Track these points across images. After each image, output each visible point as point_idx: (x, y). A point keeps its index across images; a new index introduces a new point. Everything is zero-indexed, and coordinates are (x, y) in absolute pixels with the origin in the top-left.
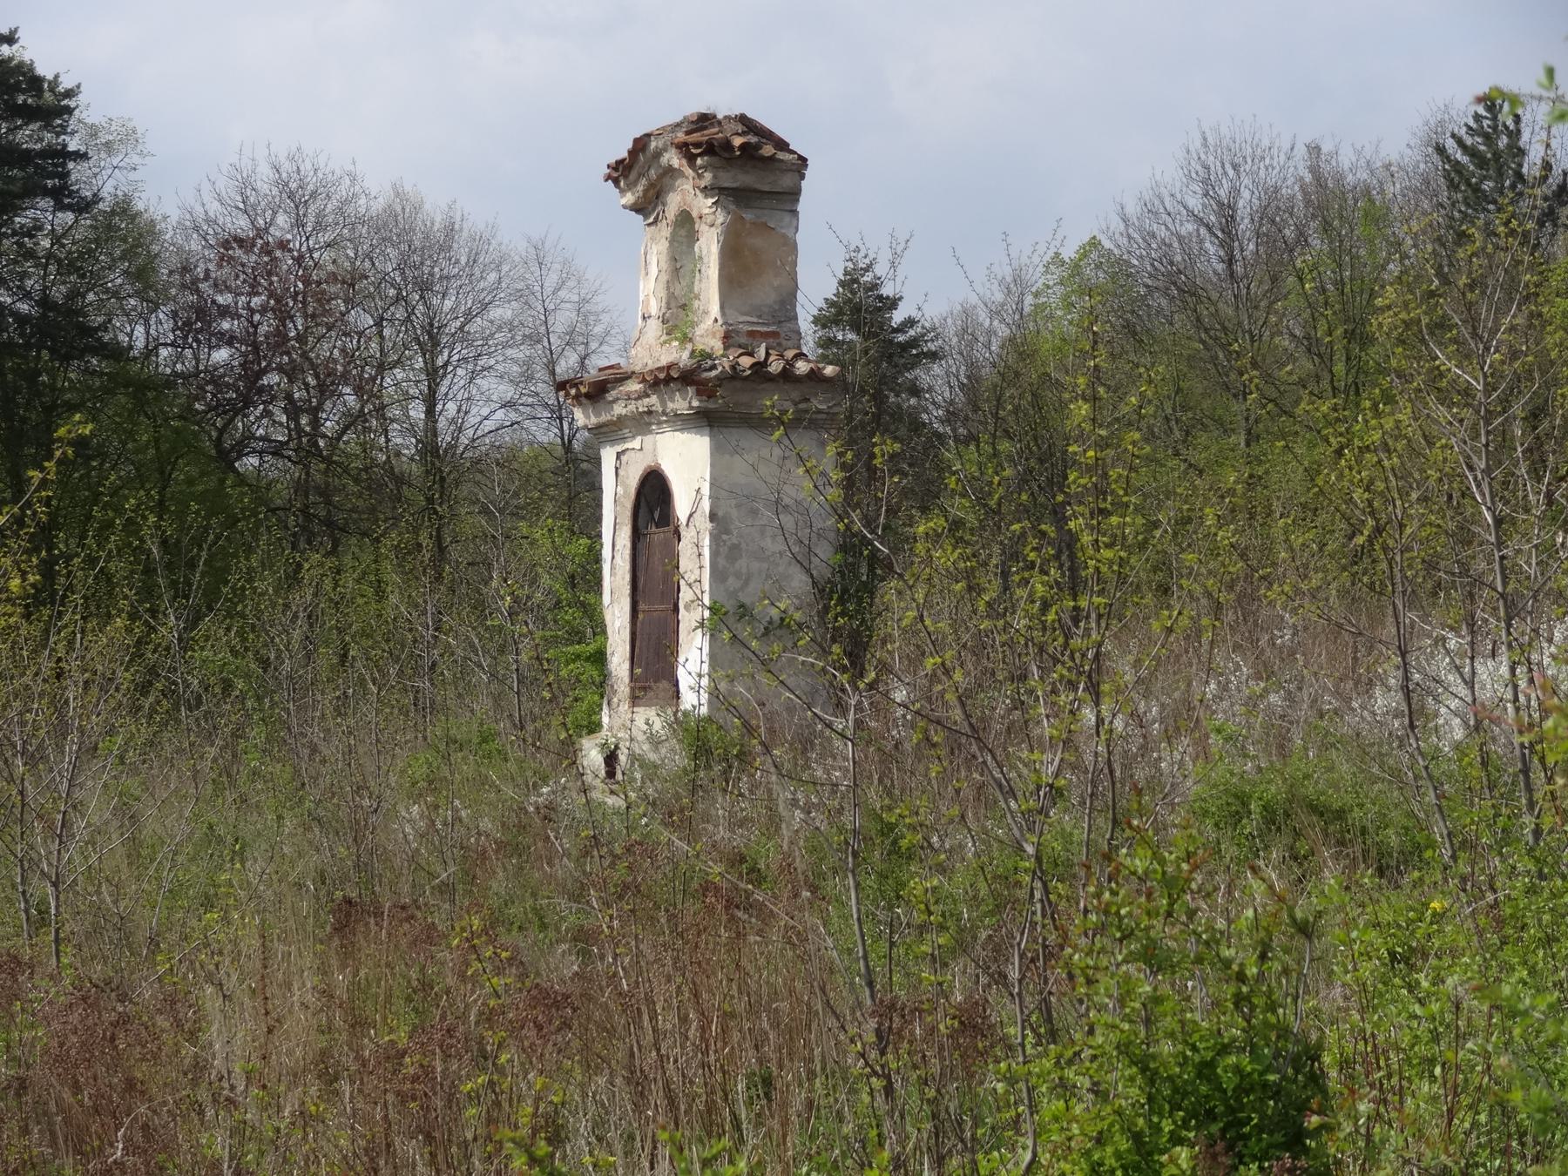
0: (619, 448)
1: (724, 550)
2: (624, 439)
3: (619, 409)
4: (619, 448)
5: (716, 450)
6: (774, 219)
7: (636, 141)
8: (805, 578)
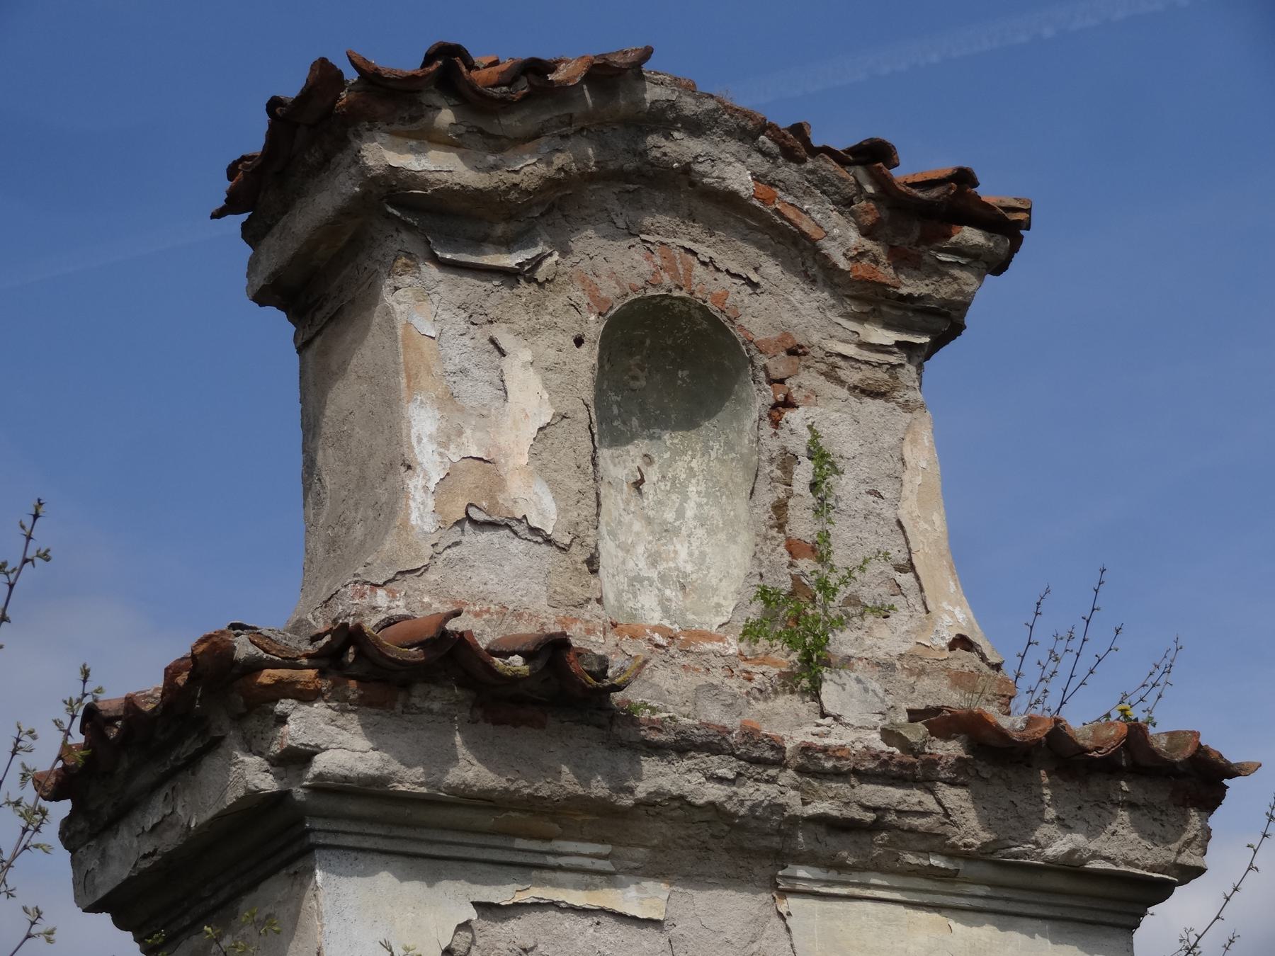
0: (503, 894)
2: (526, 869)
3: (658, 777)
4: (503, 894)
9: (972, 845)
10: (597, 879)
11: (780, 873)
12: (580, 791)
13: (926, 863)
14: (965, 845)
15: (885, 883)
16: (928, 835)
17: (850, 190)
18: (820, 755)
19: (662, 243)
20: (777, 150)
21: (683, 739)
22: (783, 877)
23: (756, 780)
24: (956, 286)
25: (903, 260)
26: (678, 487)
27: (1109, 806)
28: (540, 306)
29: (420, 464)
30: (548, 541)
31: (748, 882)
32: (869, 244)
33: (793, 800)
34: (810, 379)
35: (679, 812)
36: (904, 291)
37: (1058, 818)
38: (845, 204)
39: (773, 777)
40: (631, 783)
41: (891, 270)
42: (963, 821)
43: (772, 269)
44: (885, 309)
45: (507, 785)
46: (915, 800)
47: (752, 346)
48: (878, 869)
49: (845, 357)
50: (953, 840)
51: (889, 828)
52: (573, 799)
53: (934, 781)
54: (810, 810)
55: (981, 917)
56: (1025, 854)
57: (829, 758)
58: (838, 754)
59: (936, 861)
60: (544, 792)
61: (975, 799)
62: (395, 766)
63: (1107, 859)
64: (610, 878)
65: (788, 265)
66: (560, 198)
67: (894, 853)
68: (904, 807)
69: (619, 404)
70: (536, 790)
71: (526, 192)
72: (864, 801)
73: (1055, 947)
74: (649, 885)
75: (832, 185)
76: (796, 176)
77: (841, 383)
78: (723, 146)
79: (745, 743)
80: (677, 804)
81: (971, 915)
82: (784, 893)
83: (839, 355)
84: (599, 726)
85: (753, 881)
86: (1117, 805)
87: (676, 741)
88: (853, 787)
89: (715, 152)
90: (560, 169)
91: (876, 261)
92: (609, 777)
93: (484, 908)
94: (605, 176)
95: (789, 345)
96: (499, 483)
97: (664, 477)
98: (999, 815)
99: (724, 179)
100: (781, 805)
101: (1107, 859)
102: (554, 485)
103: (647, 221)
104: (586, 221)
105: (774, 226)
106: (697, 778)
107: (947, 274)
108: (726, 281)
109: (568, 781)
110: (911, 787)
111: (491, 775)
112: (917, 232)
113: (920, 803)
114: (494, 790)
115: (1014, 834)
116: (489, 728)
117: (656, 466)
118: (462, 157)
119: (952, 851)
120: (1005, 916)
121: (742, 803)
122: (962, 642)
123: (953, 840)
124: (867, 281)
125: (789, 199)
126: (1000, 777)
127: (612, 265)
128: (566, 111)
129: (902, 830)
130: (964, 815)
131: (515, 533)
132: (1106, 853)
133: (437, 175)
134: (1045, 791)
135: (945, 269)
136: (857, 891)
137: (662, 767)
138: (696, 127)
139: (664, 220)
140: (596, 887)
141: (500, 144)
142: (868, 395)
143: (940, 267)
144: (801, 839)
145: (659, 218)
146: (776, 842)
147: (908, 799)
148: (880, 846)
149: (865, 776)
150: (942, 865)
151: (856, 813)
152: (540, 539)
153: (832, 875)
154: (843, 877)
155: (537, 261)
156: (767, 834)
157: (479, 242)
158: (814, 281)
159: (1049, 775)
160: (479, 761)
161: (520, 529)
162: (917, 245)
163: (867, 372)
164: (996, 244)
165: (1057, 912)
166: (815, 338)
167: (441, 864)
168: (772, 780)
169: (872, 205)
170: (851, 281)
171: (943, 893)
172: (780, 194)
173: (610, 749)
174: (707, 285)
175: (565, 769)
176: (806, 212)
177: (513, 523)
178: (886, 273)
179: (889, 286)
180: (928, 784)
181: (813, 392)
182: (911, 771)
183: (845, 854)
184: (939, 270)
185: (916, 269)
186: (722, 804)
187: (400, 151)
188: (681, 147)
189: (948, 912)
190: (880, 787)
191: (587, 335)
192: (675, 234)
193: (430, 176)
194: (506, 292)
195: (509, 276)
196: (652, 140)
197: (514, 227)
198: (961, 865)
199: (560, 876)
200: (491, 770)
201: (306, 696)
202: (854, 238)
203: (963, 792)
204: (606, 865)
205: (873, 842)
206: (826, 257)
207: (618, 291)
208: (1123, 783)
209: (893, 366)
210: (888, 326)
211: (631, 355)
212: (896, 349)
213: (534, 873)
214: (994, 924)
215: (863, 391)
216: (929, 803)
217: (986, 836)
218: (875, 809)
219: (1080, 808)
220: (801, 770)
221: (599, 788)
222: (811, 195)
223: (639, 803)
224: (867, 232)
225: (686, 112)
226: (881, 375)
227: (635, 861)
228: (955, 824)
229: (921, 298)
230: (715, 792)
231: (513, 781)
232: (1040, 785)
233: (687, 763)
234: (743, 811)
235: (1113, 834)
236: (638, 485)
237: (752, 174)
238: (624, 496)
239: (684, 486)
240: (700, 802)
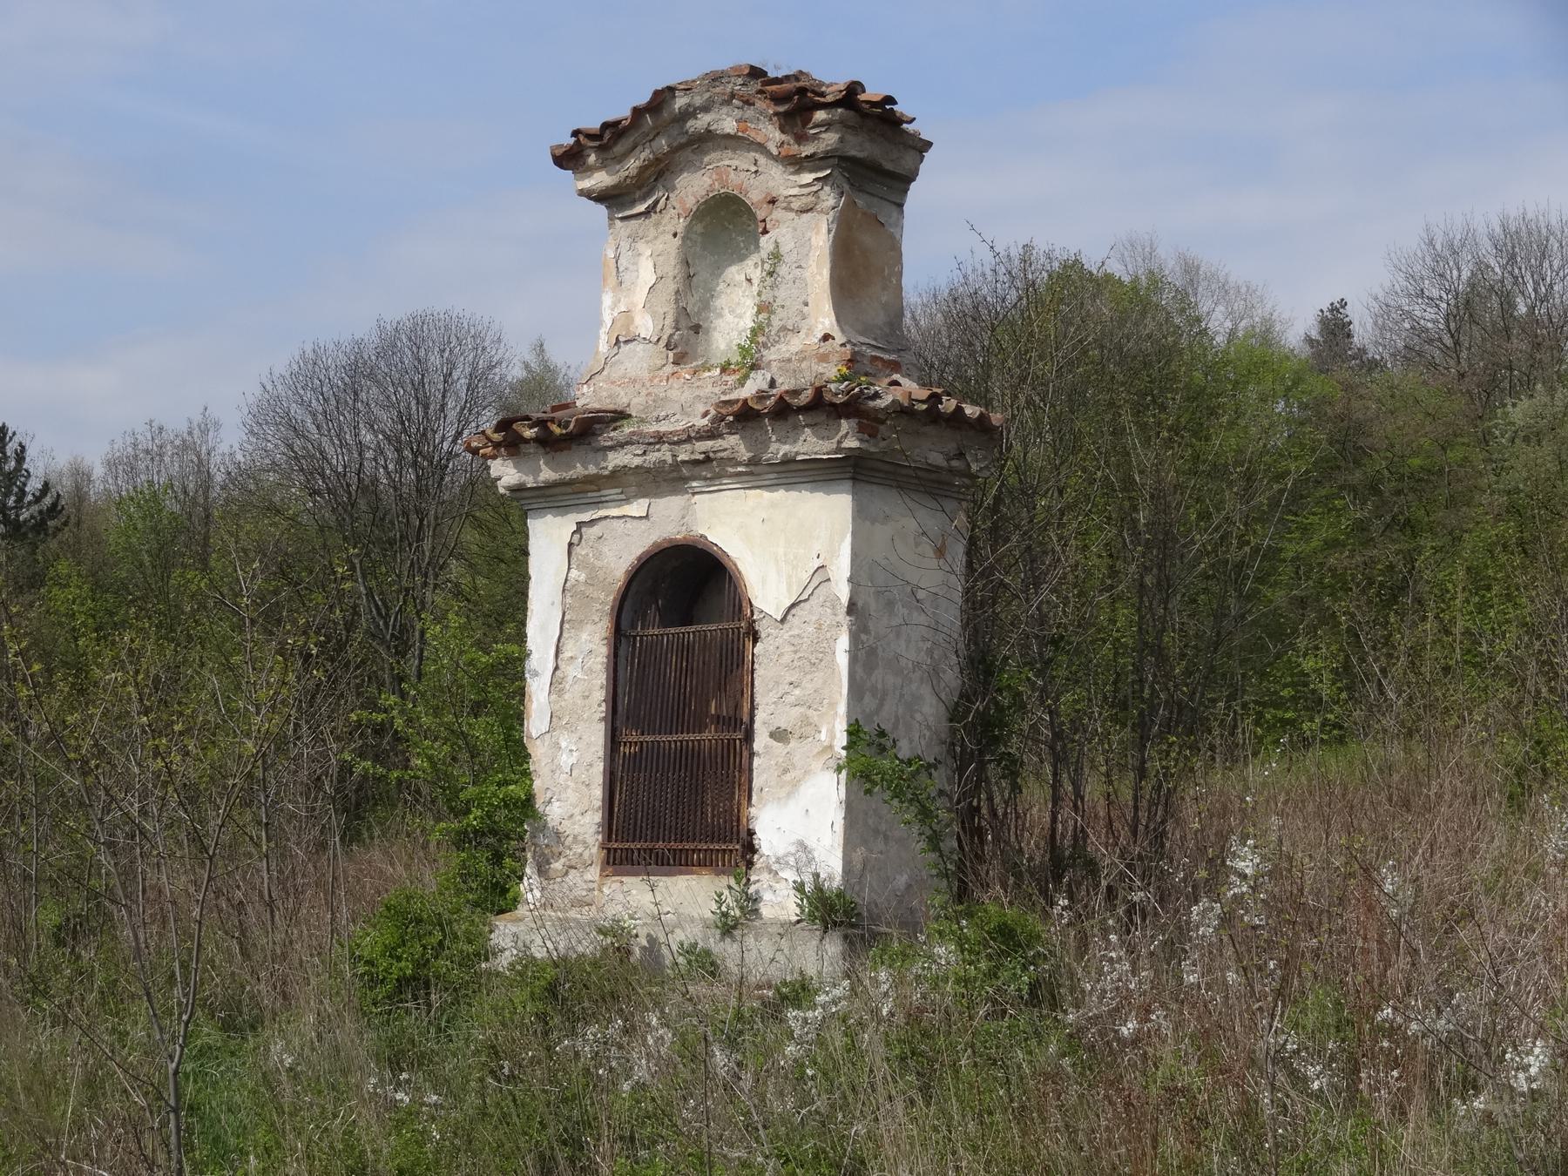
0: (586, 517)
1: (862, 655)
2: (598, 504)
3: (616, 459)
4: (586, 517)
5: (860, 514)
6: (885, 213)
7: (657, 93)
8: (934, 700)
25: (801, 139)
28: (657, 224)
34: (778, 214)
62: (524, 478)
64: (627, 500)
77: (792, 210)
93: (580, 525)
94: (675, 150)
103: (706, 159)
104: (682, 171)
106: (629, 456)
108: (743, 175)
120: (789, 486)
122: (826, 337)
127: (693, 187)
138: (706, 109)
139: (713, 155)
141: (621, 159)
155: (656, 202)
157: (633, 203)
163: (804, 200)
178: (794, 149)
182: (711, 434)
184: (815, 137)
188: (700, 123)
195: (647, 213)
197: (645, 190)
201: (494, 457)
210: (811, 171)
221: (592, 470)
223: (614, 472)
226: (811, 199)
229: (812, 156)
230: (637, 461)
236: (749, 280)
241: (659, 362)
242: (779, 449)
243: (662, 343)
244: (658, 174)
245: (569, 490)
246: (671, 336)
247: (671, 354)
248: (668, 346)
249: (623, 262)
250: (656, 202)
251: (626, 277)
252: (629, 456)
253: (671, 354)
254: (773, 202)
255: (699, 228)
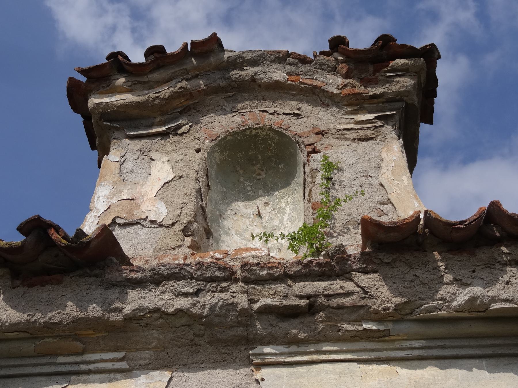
9: (389, 308)
10: (118, 375)
11: (251, 352)
12: (81, 315)
13: (361, 328)
14: (384, 309)
15: (336, 348)
16: (354, 308)
17: (334, 63)
18: (255, 268)
19: (250, 112)
20: (296, 61)
21: (155, 274)
22: (253, 355)
23: (213, 292)
24: (400, 85)
25: (366, 82)
26: (282, 211)
27: (499, 266)
29: (96, 207)
30: (161, 226)
31: (232, 363)
32: (347, 81)
33: (242, 301)
35: (161, 320)
36: (371, 93)
37: (456, 280)
38: (333, 70)
39: (225, 287)
40: (119, 305)
41: (363, 88)
42: (379, 294)
43: (306, 108)
44: (366, 106)
45: (29, 318)
46: (338, 286)
47: (296, 136)
48: (327, 340)
49: (348, 130)
50: (374, 307)
51: (324, 308)
52: (77, 321)
53: (349, 272)
54: (257, 305)
55: (424, 363)
56: (435, 308)
57: (262, 268)
58: (269, 265)
59: (367, 326)
60: (56, 320)
61: (385, 278)
63: (507, 300)
65: (314, 103)
66: (194, 104)
67: (334, 326)
68: (331, 292)
69: (250, 186)
70: (50, 319)
71: (164, 99)
72: (297, 293)
73: (492, 375)
74: (156, 374)
75: (325, 65)
76: (309, 68)
77: (347, 139)
78: (270, 67)
79: (199, 269)
80: (156, 315)
81: (416, 363)
82: (259, 366)
83: (344, 129)
84: (96, 276)
85: (235, 361)
86: (505, 264)
87: (151, 276)
88: (290, 286)
89: (266, 70)
90: (181, 88)
91: (354, 86)
92: (101, 304)
95: (317, 131)
96: (138, 206)
97: (274, 209)
98: (406, 285)
99: (271, 78)
100: (233, 304)
101: (507, 300)
102: (168, 204)
103: (240, 105)
104: (209, 112)
105: (302, 90)
107: (393, 81)
109: (71, 310)
110: (336, 280)
111: (18, 314)
112: (371, 68)
113: (342, 287)
114: (19, 323)
115: (422, 296)
116: (21, 290)
117: (270, 206)
118: (132, 95)
119: (377, 317)
120: (444, 360)
121: (204, 306)
123: (374, 307)
124: (349, 94)
125: (307, 77)
126: (401, 261)
128: (182, 68)
129: (333, 308)
130: (380, 291)
131: (143, 226)
132: (504, 296)
133: (118, 102)
134: (440, 264)
135: (392, 79)
136: (315, 357)
137: (143, 294)
138: (254, 62)
140: (117, 380)
142: (363, 141)
143: (388, 79)
144: (259, 326)
145: (246, 103)
146: (240, 331)
147: (332, 286)
148: (322, 322)
149: (297, 277)
150: (374, 328)
151: (294, 302)
152: (156, 226)
153: (293, 348)
154: (302, 349)
156: (232, 327)
158: (328, 106)
159: (440, 254)
160: (12, 307)
161: (146, 223)
162: (374, 75)
163: (361, 132)
164: (415, 62)
165: (489, 351)
166: (331, 126)
167: (9, 380)
168: (225, 290)
169: (344, 64)
170: (342, 97)
171: (386, 350)
172: (301, 76)
173: (106, 289)
174: (270, 120)
175: (70, 303)
176: (316, 79)
177: (141, 221)
178: (360, 89)
179: (362, 93)
180: (347, 275)
181: (330, 145)
183: (295, 331)
184: (388, 80)
185: (376, 84)
186: (188, 309)
187: (102, 98)
188: (249, 72)
189: (395, 363)
190: (309, 283)
191: (202, 147)
192: (257, 107)
193: (115, 103)
194: (163, 141)
196: (232, 73)
197: (167, 117)
198: (390, 326)
199: (92, 377)
200: (18, 311)
202: (340, 81)
203: (376, 276)
204: (123, 365)
205: (316, 321)
206: (327, 92)
207: (223, 131)
208: (503, 248)
209: (376, 127)
210: (370, 112)
211: (254, 165)
212: (377, 120)
213: (74, 378)
214: (437, 366)
215: (359, 140)
216: (350, 286)
217: (398, 300)
218: (308, 297)
219: (474, 271)
220: (246, 281)
221: (94, 311)
222: (317, 72)
223: (128, 319)
224: (346, 76)
225: (248, 58)
227: (144, 359)
228: (373, 297)
229: (382, 95)
231: (33, 316)
232: (435, 261)
233: (161, 289)
234: (205, 312)
235: (508, 283)
236: (259, 215)
237: (286, 74)
238: (251, 220)
239: (284, 209)
240: (171, 310)
241: (173, 244)
242: (457, 295)
243: (178, 228)
244: (188, 107)
245: (29, 347)
246: (190, 222)
247: (188, 241)
248: (185, 231)
249: (128, 166)
250: (180, 127)
251: (131, 177)
252: (168, 296)
253: (188, 241)
254: (322, 133)
255: (217, 156)
